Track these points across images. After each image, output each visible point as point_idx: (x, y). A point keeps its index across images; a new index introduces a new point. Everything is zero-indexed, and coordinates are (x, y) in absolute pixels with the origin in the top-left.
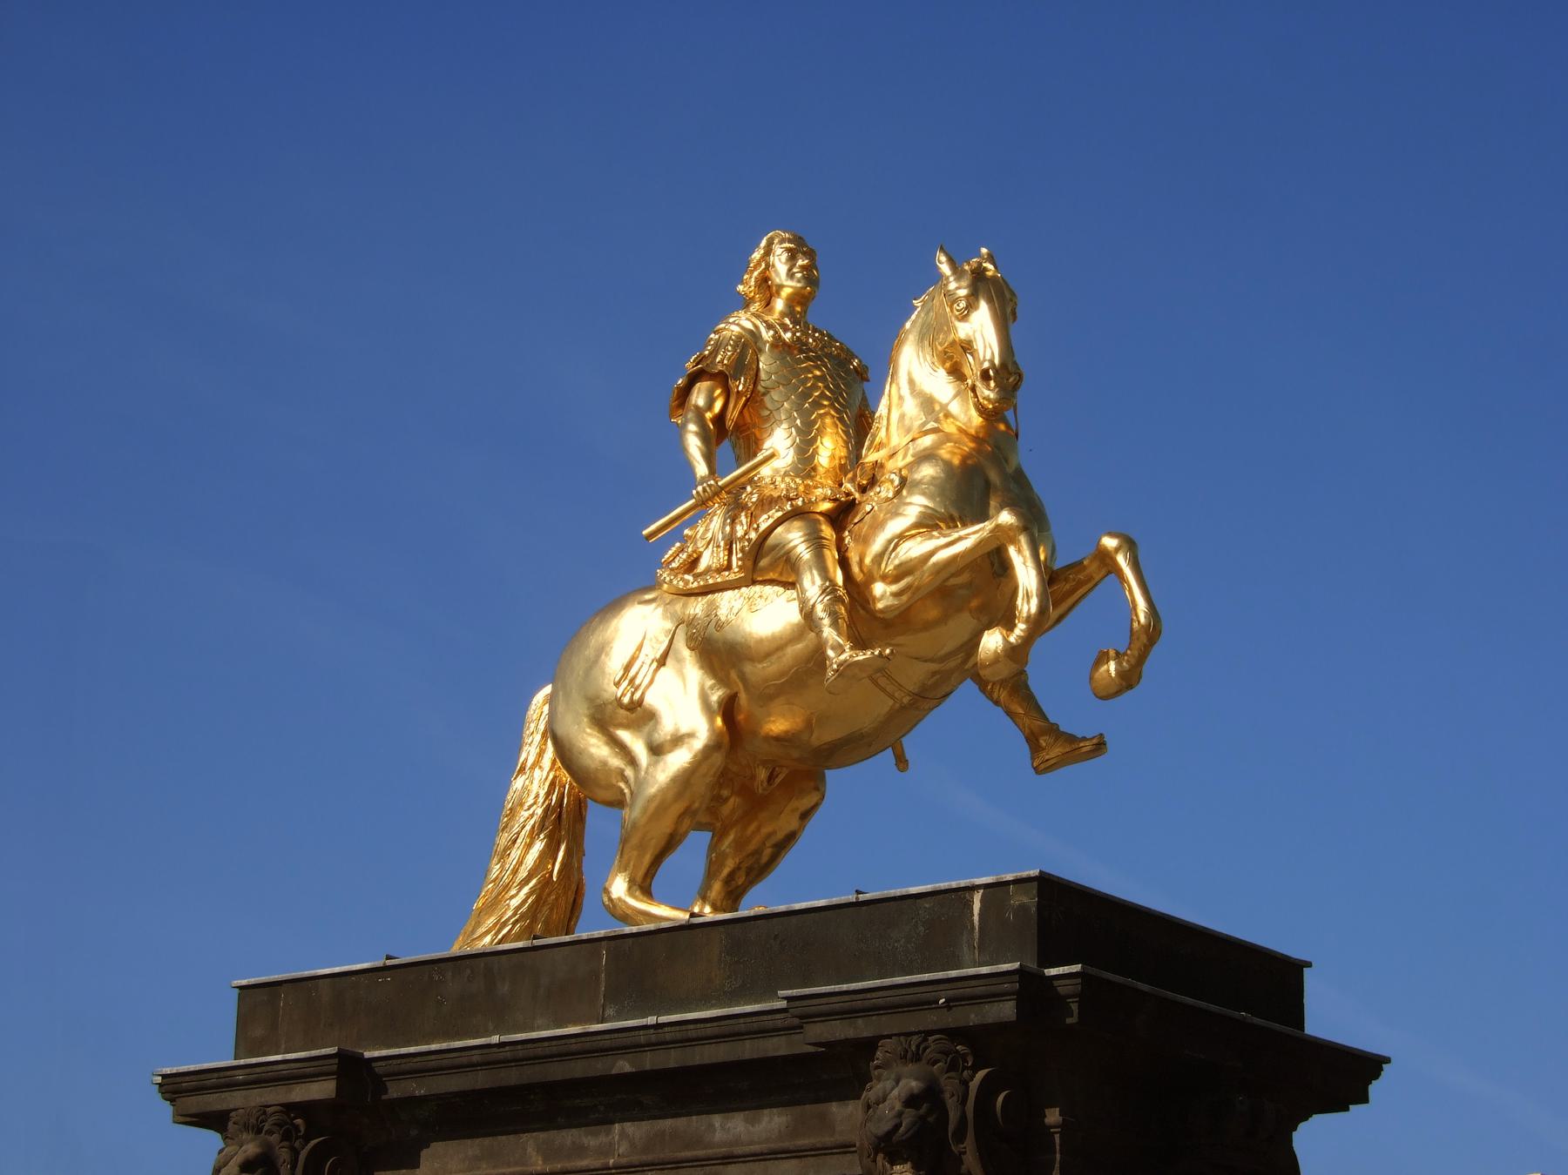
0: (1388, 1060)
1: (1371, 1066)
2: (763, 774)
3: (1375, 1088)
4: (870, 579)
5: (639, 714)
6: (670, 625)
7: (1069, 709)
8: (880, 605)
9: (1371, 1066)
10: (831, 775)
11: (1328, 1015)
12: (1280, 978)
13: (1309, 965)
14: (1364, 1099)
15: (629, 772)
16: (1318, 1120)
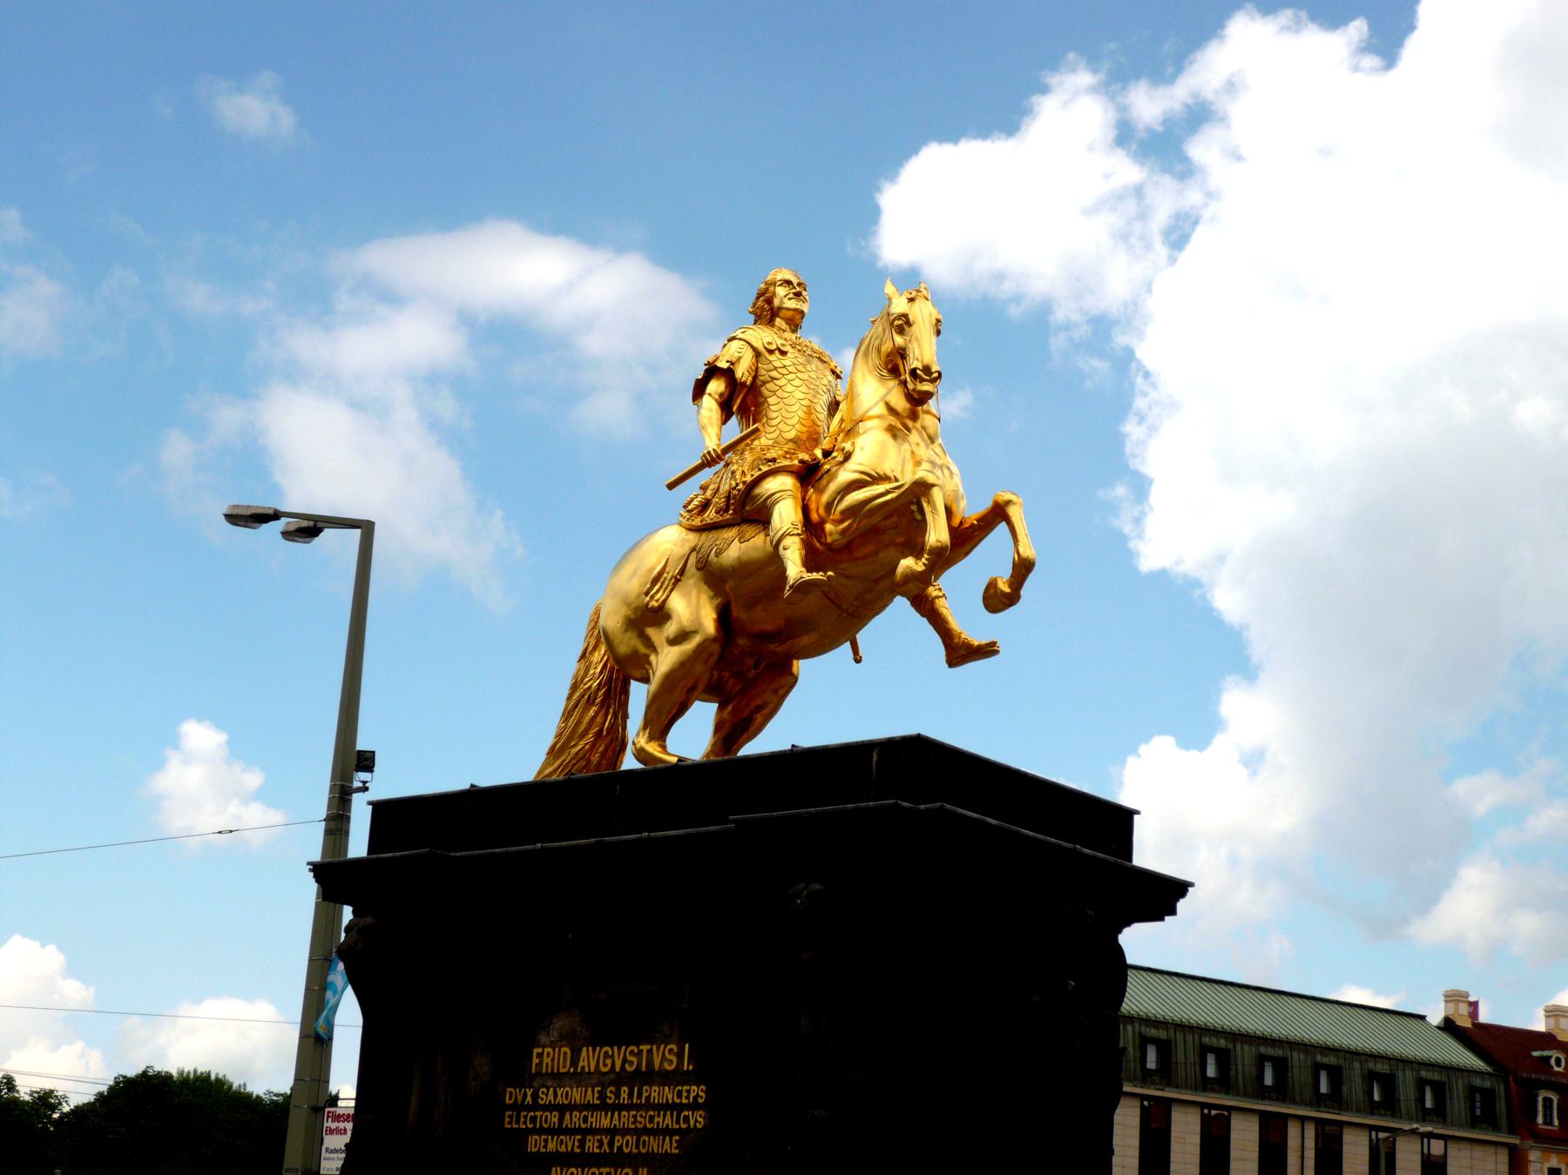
0: (1192, 885)
1: (1178, 888)
2: (750, 662)
3: (1181, 905)
4: (823, 522)
5: (660, 615)
6: (687, 549)
7: (971, 623)
8: (829, 540)
9: (1178, 888)
10: (803, 667)
11: (1150, 851)
12: (1115, 823)
13: (1138, 812)
14: (1173, 912)
15: (653, 658)
16: (1126, 931)
